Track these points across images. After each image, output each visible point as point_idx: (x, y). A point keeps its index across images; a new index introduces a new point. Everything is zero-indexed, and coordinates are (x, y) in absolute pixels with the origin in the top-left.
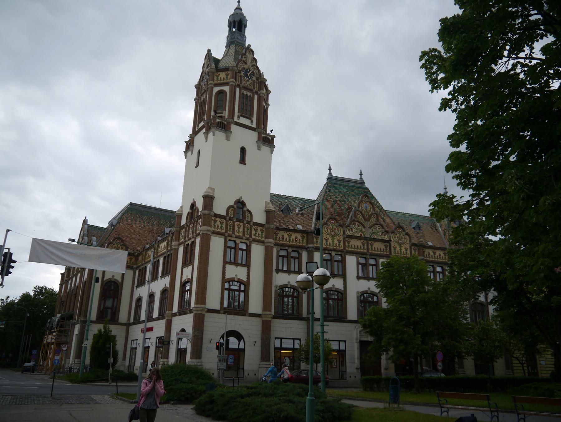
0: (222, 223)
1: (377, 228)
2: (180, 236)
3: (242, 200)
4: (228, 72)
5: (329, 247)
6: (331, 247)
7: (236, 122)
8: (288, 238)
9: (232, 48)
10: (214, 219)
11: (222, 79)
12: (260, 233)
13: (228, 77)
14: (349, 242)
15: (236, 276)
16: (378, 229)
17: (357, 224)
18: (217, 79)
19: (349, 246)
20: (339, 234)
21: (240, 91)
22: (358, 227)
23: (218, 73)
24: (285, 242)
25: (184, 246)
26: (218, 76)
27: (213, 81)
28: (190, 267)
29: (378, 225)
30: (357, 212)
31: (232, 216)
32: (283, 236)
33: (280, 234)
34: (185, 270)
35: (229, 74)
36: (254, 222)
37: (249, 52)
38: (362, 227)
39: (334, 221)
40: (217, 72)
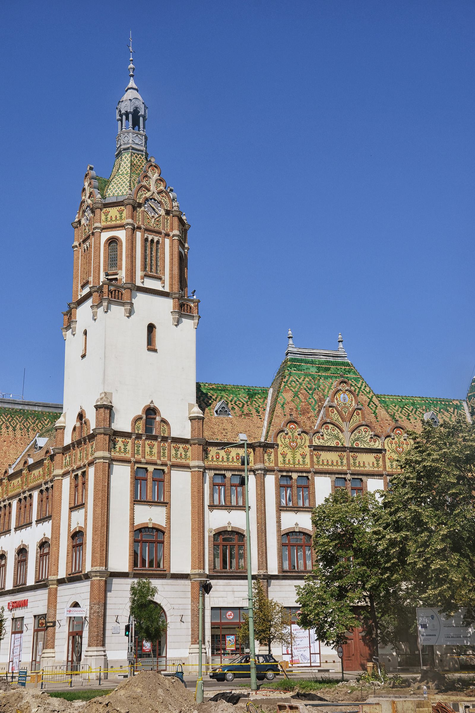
0: (125, 445)
1: (363, 430)
2: (64, 462)
3: (154, 406)
5: (288, 466)
6: (291, 466)
7: (138, 287)
8: (225, 457)
9: (125, 160)
10: (113, 439)
11: (114, 219)
12: (183, 453)
13: (123, 215)
14: (318, 457)
15: (150, 520)
16: (364, 433)
17: (330, 428)
19: (318, 461)
20: (302, 444)
21: (143, 236)
22: (332, 432)
23: (107, 209)
24: (221, 463)
25: (71, 477)
26: (106, 214)
27: (100, 222)
28: (82, 511)
30: (330, 409)
31: (140, 432)
32: (218, 454)
33: (213, 451)
34: (74, 514)
36: (173, 438)
37: (153, 170)
38: (339, 431)
39: (295, 426)
40: (104, 208)
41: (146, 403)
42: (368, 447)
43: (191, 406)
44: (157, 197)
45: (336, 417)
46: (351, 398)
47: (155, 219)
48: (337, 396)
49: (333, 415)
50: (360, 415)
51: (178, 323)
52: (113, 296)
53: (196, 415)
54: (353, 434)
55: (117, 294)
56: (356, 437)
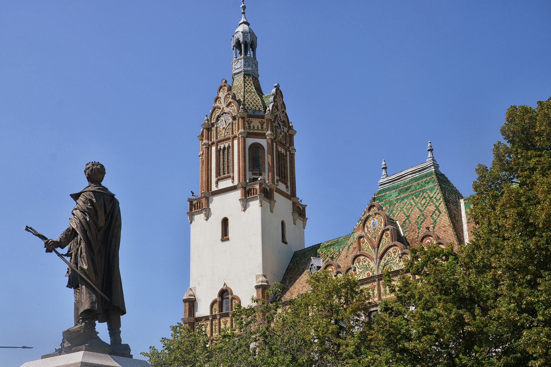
16: (393, 254)
17: (361, 260)
29: (393, 248)
30: (361, 240)
38: (370, 261)
41: (221, 287)
42: (398, 269)
43: (257, 277)
44: (227, 110)
45: (366, 247)
46: (380, 221)
47: (225, 130)
48: (368, 224)
49: (364, 245)
50: (389, 236)
51: (245, 208)
52: (196, 208)
53: (260, 284)
54: (383, 261)
55: (199, 205)
56: (386, 261)
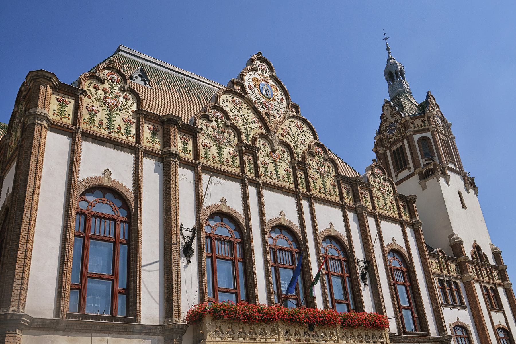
4: (424, 118)
11: (419, 126)
18: (414, 126)
23: (413, 120)
35: (426, 120)
